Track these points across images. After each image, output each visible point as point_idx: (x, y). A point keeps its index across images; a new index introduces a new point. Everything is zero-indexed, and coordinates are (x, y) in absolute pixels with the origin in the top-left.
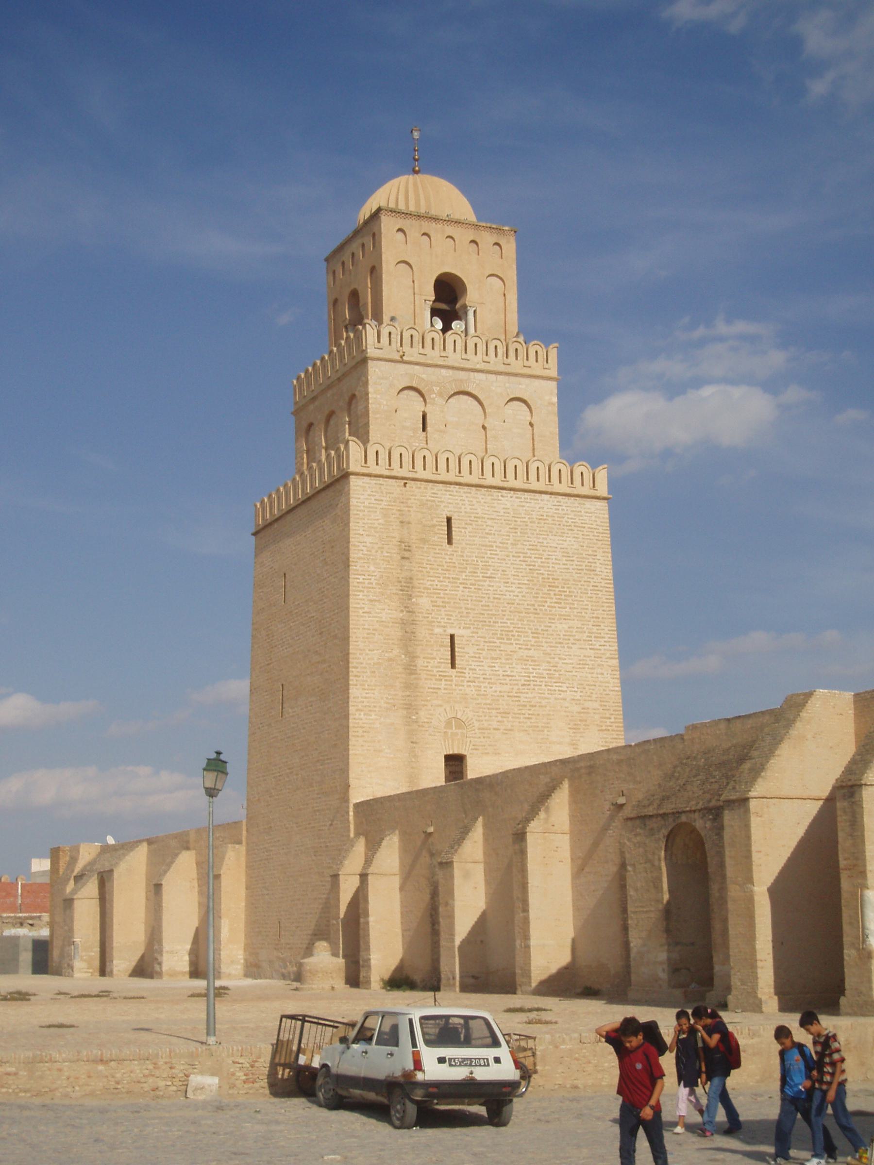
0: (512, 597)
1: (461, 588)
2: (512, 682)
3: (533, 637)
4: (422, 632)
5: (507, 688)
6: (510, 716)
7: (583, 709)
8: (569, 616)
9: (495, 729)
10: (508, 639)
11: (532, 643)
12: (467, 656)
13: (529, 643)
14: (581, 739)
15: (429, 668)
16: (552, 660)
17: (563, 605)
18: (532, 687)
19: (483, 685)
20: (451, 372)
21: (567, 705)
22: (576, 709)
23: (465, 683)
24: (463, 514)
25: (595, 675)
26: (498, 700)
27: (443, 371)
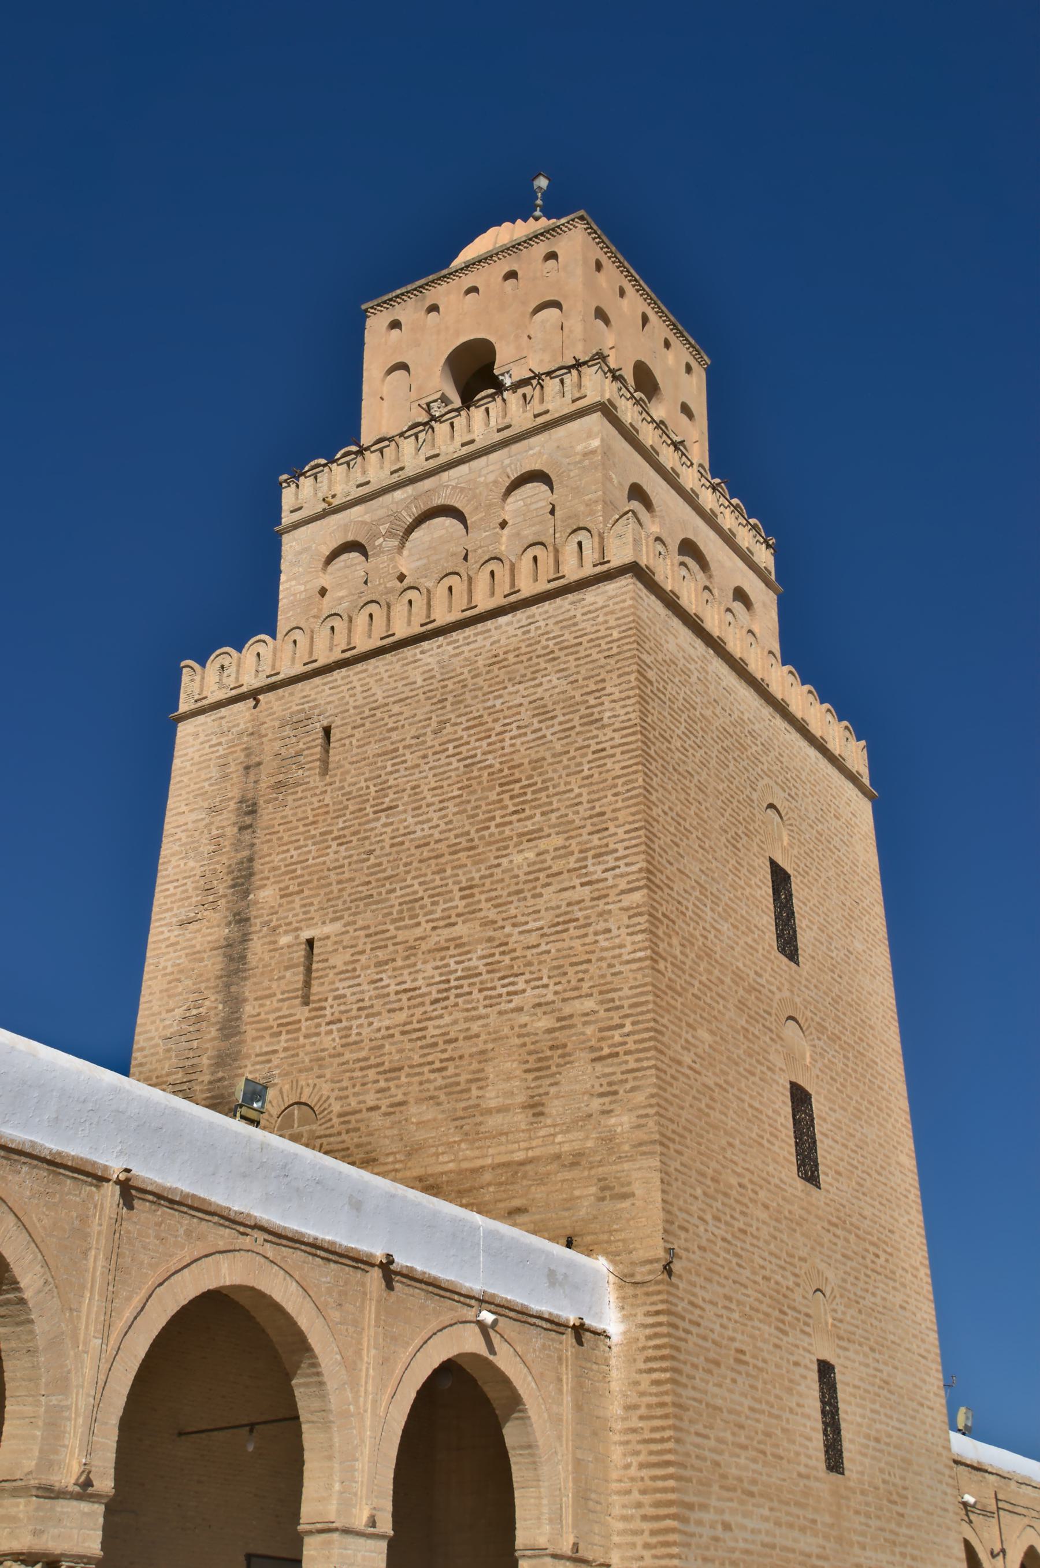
0: (427, 832)
1: (334, 844)
2: (413, 1002)
3: (463, 898)
4: (257, 949)
5: (401, 1017)
6: (403, 1074)
7: (559, 1020)
8: (541, 830)
9: (371, 1109)
10: (411, 917)
11: (460, 910)
12: (331, 973)
13: (453, 912)
14: (553, 1090)
15: (263, 1016)
16: (498, 934)
17: (528, 813)
18: (452, 1000)
19: (355, 1023)
20: (409, 490)
21: (524, 1019)
22: (545, 1022)
23: (324, 1029)
24: (352, 711)
25: (587, 940)
26: (382, 1046)
27: (398, 494)
